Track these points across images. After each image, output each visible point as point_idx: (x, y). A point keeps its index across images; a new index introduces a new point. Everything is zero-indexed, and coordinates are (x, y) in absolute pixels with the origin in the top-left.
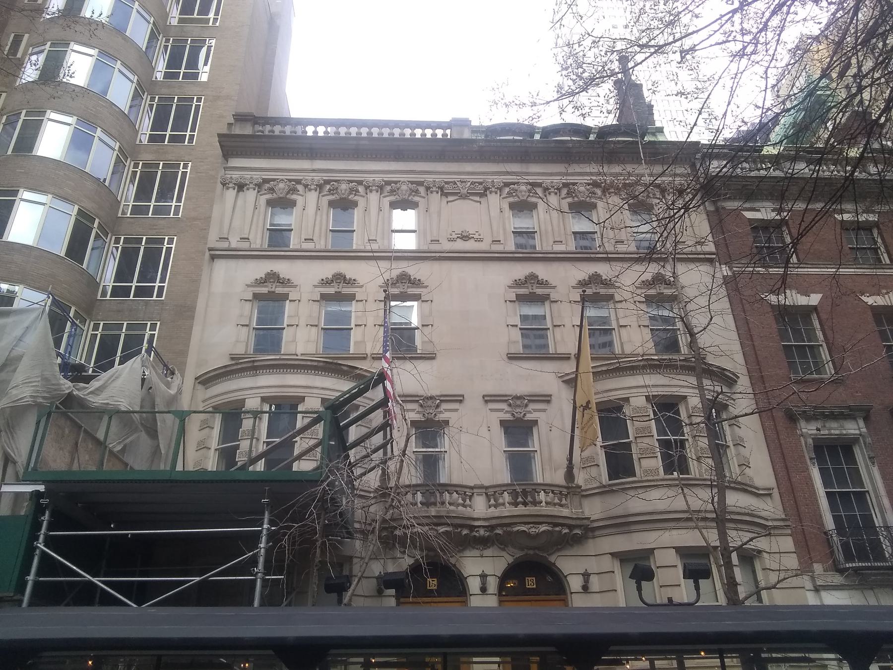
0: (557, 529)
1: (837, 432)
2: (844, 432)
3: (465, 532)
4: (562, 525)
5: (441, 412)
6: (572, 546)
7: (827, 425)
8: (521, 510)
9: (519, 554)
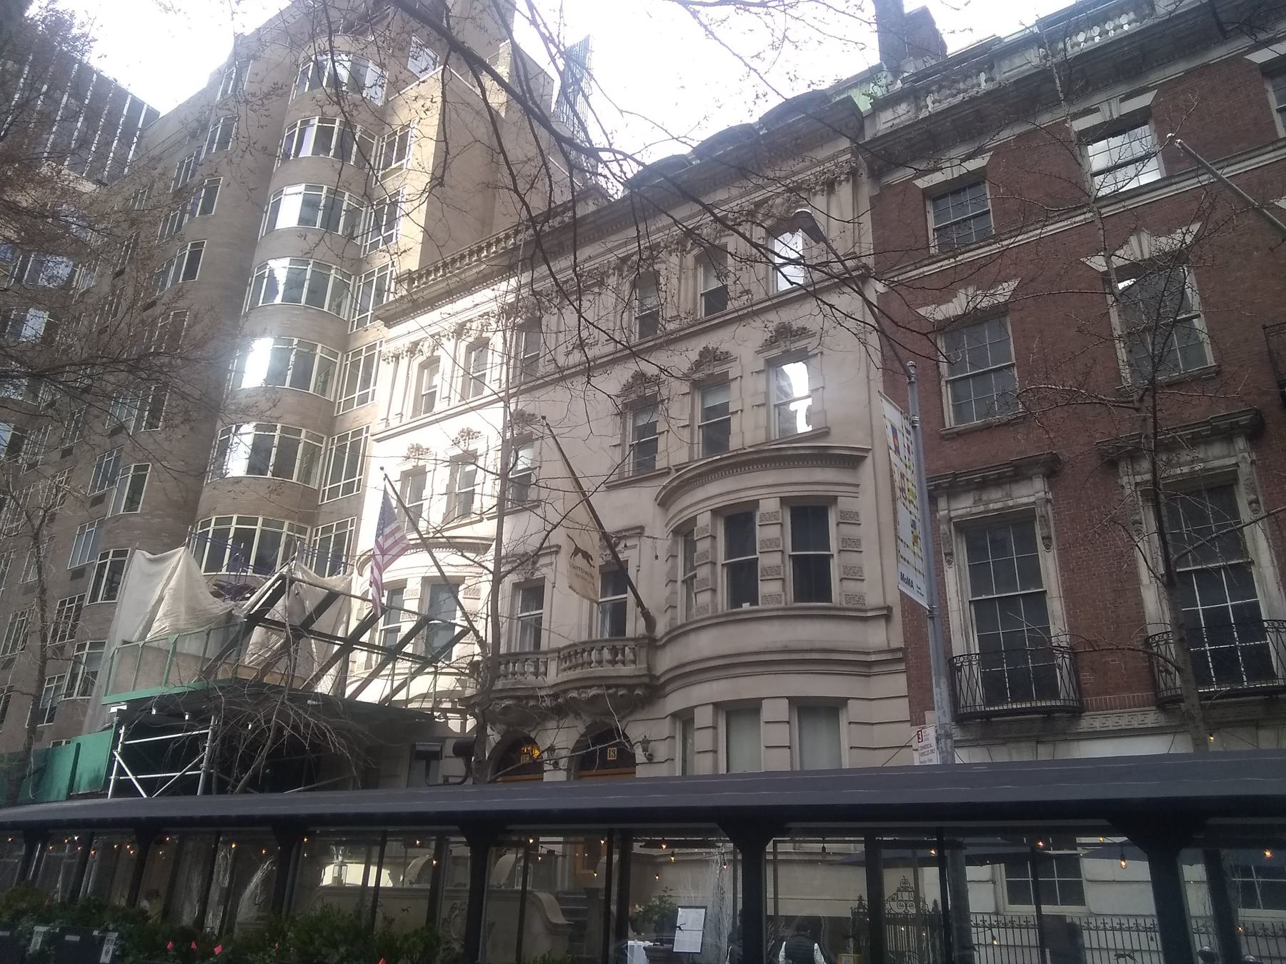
0: (611, 691)
1: (999, 505)
2: (1011, 503)
3: (532, 703)
4: (617, 686)
5: (538, 569)
6: (643, 708)
7: (985, 497)
8: (572, 675)
9: (589, 721)
